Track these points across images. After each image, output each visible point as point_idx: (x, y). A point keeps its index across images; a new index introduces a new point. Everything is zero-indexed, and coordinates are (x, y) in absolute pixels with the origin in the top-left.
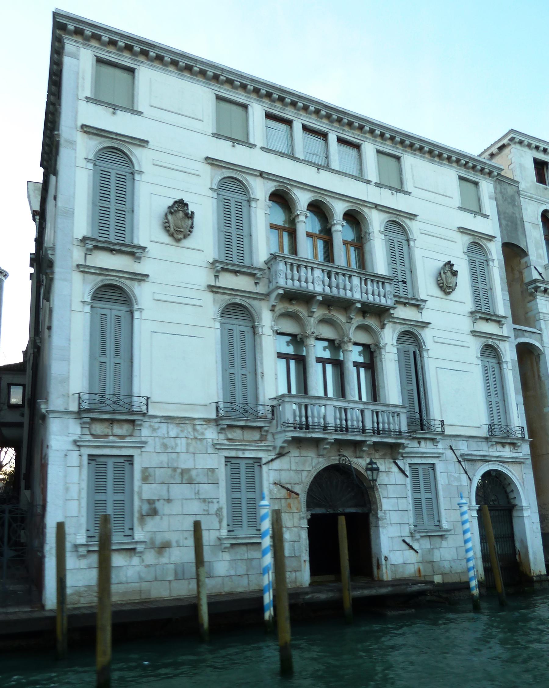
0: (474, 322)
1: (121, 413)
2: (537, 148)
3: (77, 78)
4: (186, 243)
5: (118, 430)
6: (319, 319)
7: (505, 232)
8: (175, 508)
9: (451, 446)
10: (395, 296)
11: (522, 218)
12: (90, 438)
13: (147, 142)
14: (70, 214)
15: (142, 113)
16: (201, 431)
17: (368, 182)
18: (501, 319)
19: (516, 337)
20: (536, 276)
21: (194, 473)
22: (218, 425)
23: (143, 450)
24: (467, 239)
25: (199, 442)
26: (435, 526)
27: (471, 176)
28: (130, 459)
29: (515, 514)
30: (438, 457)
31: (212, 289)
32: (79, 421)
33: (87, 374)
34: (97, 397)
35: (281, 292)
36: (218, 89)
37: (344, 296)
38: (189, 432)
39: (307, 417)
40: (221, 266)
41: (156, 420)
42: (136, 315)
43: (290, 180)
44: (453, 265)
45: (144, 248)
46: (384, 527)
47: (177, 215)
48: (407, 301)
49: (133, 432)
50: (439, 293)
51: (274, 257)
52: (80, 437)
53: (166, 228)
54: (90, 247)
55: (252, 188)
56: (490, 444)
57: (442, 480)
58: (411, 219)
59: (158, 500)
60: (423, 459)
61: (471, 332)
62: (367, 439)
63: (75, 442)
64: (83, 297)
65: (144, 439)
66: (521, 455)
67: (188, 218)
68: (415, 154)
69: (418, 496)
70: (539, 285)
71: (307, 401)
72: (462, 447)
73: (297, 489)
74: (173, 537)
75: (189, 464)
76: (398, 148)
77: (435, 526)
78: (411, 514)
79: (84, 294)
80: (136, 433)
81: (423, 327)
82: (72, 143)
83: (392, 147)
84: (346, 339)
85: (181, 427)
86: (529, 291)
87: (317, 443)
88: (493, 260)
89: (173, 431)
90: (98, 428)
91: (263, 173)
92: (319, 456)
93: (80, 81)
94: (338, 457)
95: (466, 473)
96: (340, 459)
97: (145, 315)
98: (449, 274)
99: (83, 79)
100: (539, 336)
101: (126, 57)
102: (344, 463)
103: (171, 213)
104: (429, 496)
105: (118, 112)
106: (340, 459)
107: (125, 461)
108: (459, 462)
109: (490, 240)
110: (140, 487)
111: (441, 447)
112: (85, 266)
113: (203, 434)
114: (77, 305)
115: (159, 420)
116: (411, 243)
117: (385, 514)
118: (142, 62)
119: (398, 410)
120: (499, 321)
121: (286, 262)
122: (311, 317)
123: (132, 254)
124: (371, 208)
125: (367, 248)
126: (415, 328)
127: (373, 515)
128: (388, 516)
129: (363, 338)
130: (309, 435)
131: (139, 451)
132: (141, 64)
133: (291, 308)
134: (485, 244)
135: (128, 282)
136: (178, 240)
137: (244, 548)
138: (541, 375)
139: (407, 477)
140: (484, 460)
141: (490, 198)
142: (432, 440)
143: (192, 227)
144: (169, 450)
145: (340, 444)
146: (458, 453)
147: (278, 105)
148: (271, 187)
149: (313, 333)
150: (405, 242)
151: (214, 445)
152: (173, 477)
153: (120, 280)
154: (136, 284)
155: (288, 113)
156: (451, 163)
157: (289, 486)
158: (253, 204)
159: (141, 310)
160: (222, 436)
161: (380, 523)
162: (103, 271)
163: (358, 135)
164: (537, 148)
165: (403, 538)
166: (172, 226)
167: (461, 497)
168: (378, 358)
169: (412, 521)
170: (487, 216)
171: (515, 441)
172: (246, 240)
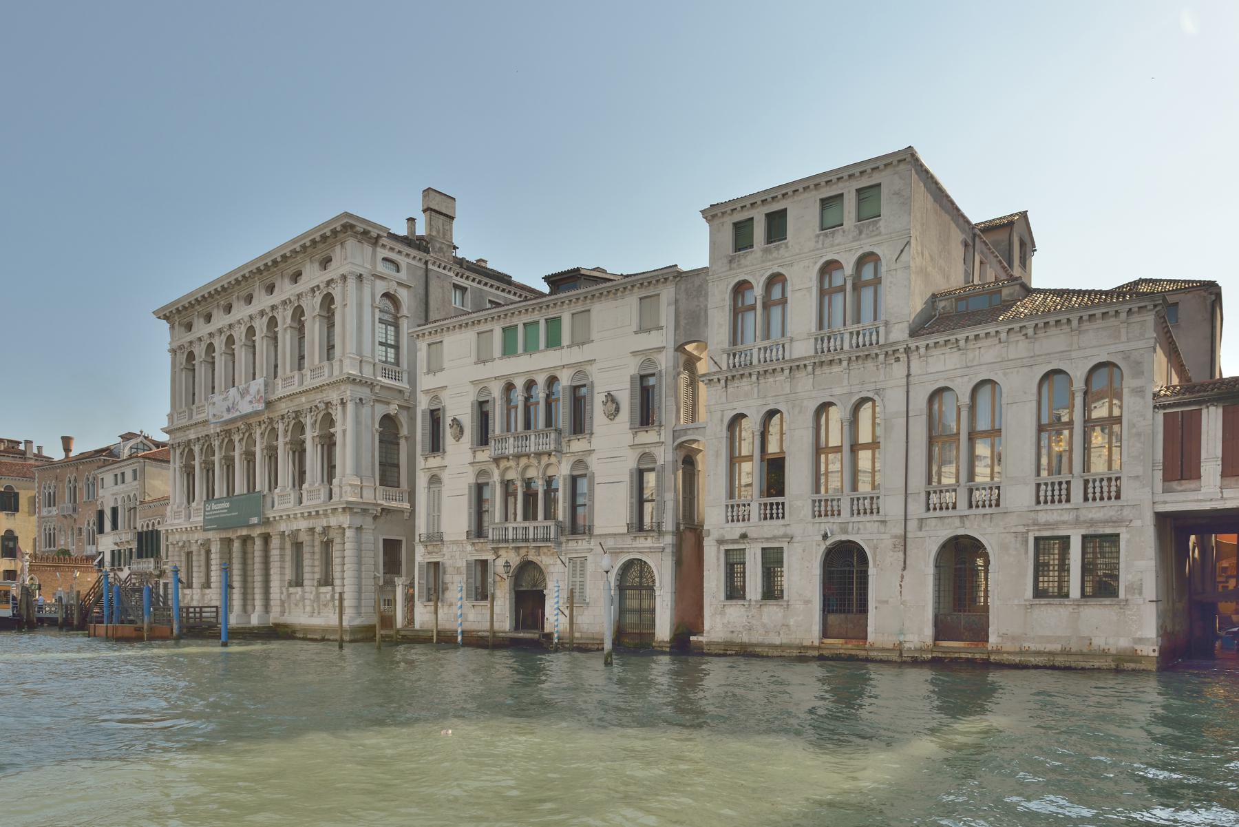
66: (662, 545)
72: (610, 543)
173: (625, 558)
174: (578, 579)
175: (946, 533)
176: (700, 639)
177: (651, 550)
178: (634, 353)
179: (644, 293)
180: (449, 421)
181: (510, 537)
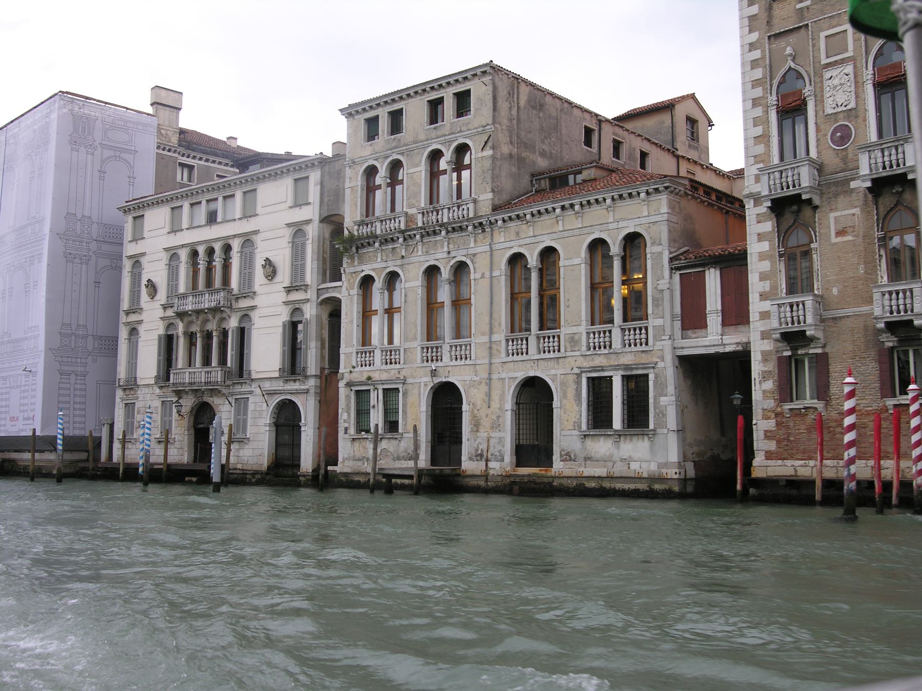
2: (364, 109)
14: (123, 299)
57: (251, 407)
66: (307, 387)
69: (245, 417)
72: (267, 386)
90: (128, 392)
111: (254, 387)
164: (364, 109)
175: (521, 375)
176: (335, 468)
177: (297, 392)
178: (289, 225)
179: (297, 176)
180: (144, 282)
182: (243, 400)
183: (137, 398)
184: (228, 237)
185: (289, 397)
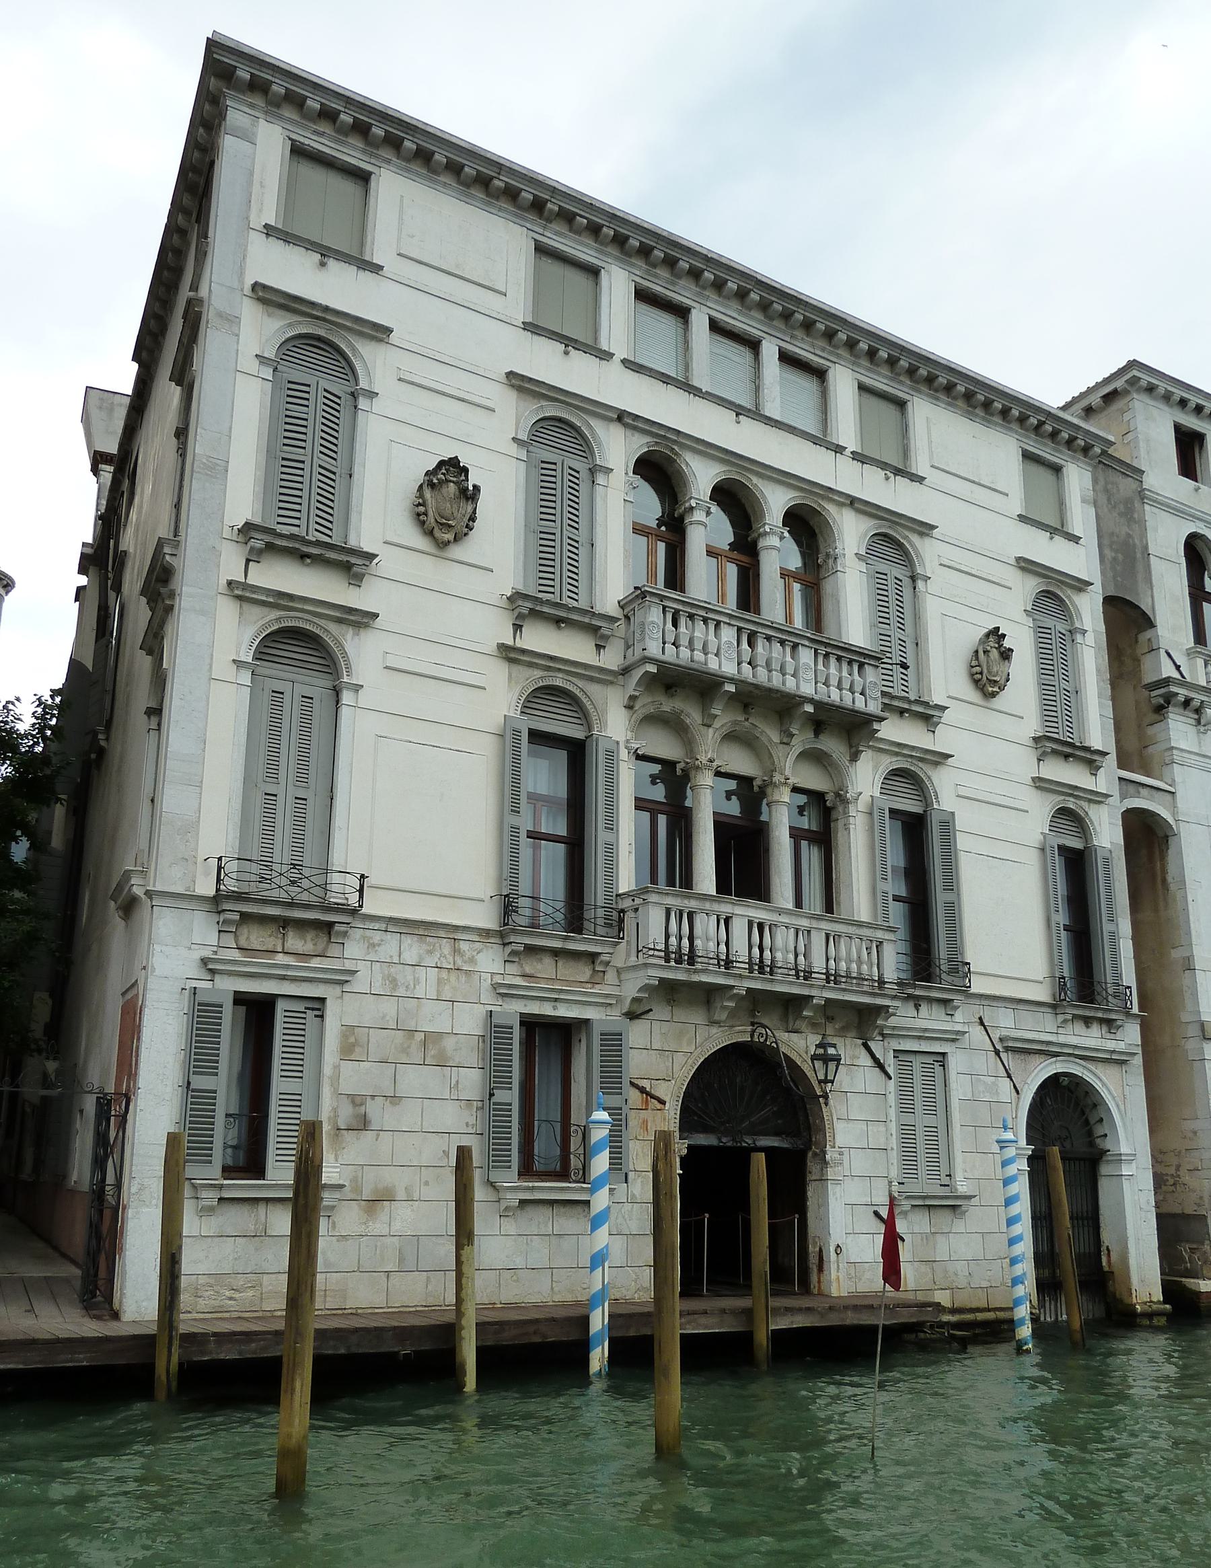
0: (1039, 760)
1: (307, 907)
2: (1183, 403)
3: (250, 183)
4: (456, 551)
5: (294, 942)
6: (725, 731)
7: (1110, 574)
8: (408, 1116)
9: (980, 1018)
10: (884, 694)
11: (1146, 547)
12: (236, 955)
13: (389, 331)
15: (381, 268)
16: (468, 954)
17: (839, 449)
18: (1095, 757)
19: (1123, 797)
20: (1168, 671)
21: (449, 1043)
22: (504, 945)
23: (347, 988)
24: (1032, 585)
25: (463, 978)
26: (941, 1185)
27: (1046, 452)
28: (318, 1004)
29: (1104, 1169)
30: (953, 1040)
31: (510, 654)
32: (215, 918)
33: (237, 818)
34: (255, 868)
35: (653, 669)
36: (541, 231)
37: (766, 684)
38: (442, 956)
39: (691, 939)
40: (529, 605)
41: (377, 926)
42: (347, 697)
43: (678, 432)
44: (1004, 636)
45: (371, 557)
46: (837, 1182)
47: (444, 490)
48: (906, 706)
49: (326, 949)
50: (972, 695)
51: (640, 595)
52: (215, 953)
53: (420, 518)
54: (259, 545)
55: (600, 444)
56: (1061, 1018)
57: (959, 1088)
58: (922, 534)
59: (373, 1097)
60: (922, 1042)
61: (1033, 779)
62: (814, 992)
63: (204, 961)
64: (238, 653)
65: (349, 965)
66: (1121, 1046)
67: (467, 499)
68: (937, 399)
69: (908, 1118)
70: (1174, 689)
71: (693, 904)
72: (1005, 1022)
73: (662, 1090)
74: (398, 1180)
75: (442, 1025)
76: (901, 382)
77: (941, 1185)
78: (894, 1156)
79: (239, 646)
80: (334, 950)
81: (937, 764)
82: (232, 320)
83: (891, 379)
84: (777, 778)
85: (429, 944)
86: (1154, 701)
87: (708, 995)
88: (1084, 632)
89: (412, 949)
90: (256, 937)
91: (626, 414)
92: (713, 1023)
93: (256, 188)
94: (750, 1028)
95: (1009, 1076)
96: (753, 1032)
97: (364, 698)
98: (995, 654)
99: (262, 186)
100: (1168, 796)
101: (355, 148)
102: (762, 1040)
103: (432, 486)
104: (930, 1120)
105: (331, 263)
106: (753, 1032)
107: (306, 1008)
108: (997, 1053)
109: (1080, 590)
110: (337, 1067)
111: (962, 1018)
112: (245, 586)
113: (472, 960)
114: (222, 666)
115: (383, 926)
116: (920, 584)
117: (841, 1154)
118: (388, 161)
119: (880, 934)
120: (1089, 759)
121: (664, 607)
122: (709, 726)
123: (346, 567)
124: (842, 505)
125: (827, 586)
126: (920, 764)
127: (815, 1154)
128: (846, 1158)
129: (814, 780)
130: (696, 978)
131: (338, 989)
132: (383, 165)
133: (668, 705)
134: (1069, 597)
135: (333, 627)
136: (443, 545)
137: (546, 1211)
138: (1169, 879)
139: (890, 1078)
140: (1047, 1052)
141: (1084, 501)
142: (945, 1002)
143: (473, 518)
144: (401, 992)
145: (757, 1002)
146: (995, 1036)
147: (663, 273)
148: (639, 445)
149: (711, 761)
150: (906, 581)
151: (495, 986)
152: (405, 1050)
153: (316, 620)
154: (350, 631)
155: (682, 293)
156: (1009, 422)
157: (645, 1084)
158: (601, 479)
159: (357, 688)
160: (512, 969)
161: (831, 1173)
162: (281, 600)
163: (823, 350)
164: (1183, 403)
165: (876, 1208)
166: (430, 513)
167: (1005, 1128)
168: (840, 823)
169: (894, 1173)
170: (1075, 539)
171: (1114, 1017)
172: (583, 552)
173: (1045, 1070)
174: (921, 1120)
181: (818, 964)
182: (917, 1061)
183: (342, 979)
184: (828, 492)
185: (1076, 1069)
